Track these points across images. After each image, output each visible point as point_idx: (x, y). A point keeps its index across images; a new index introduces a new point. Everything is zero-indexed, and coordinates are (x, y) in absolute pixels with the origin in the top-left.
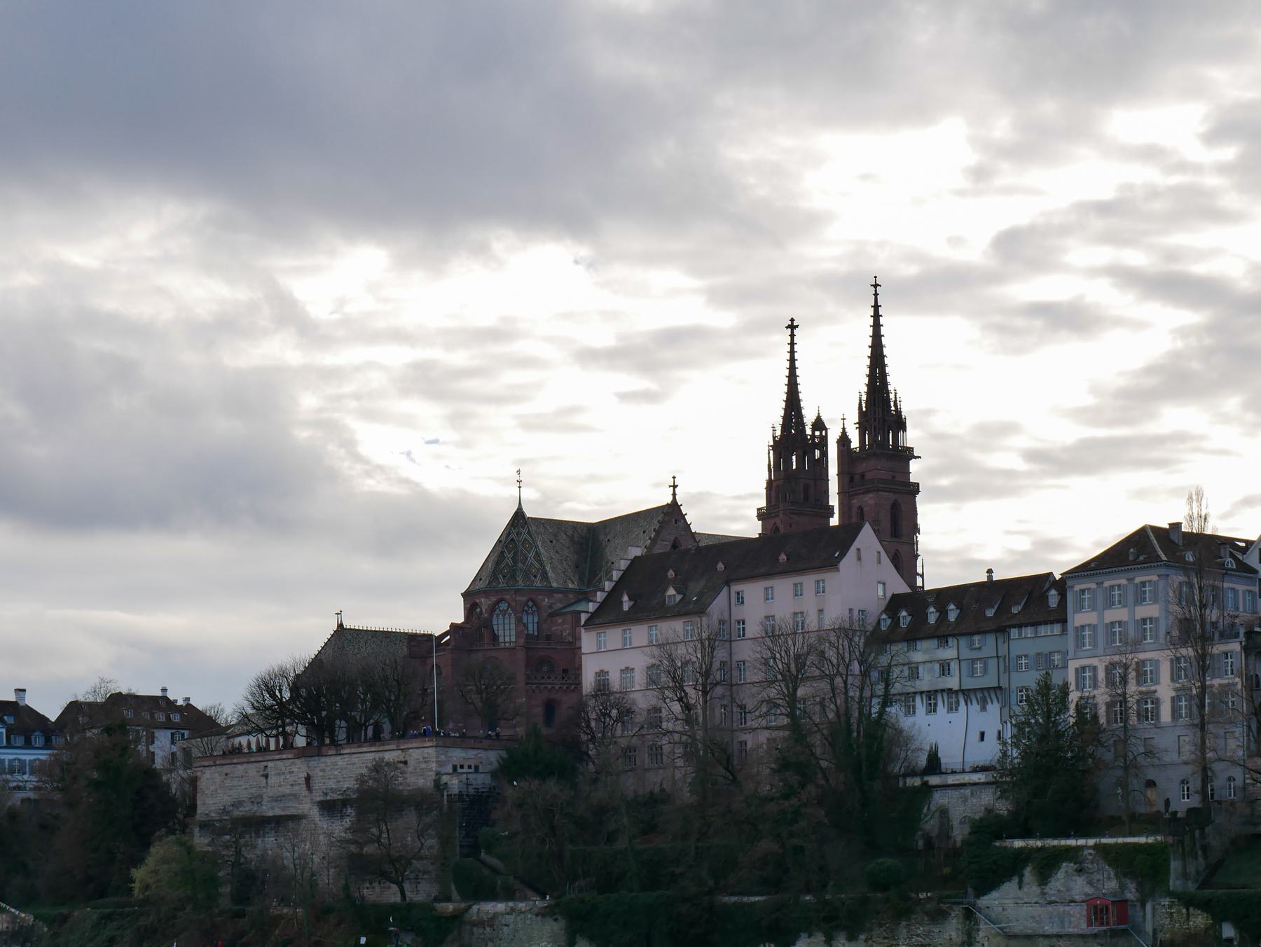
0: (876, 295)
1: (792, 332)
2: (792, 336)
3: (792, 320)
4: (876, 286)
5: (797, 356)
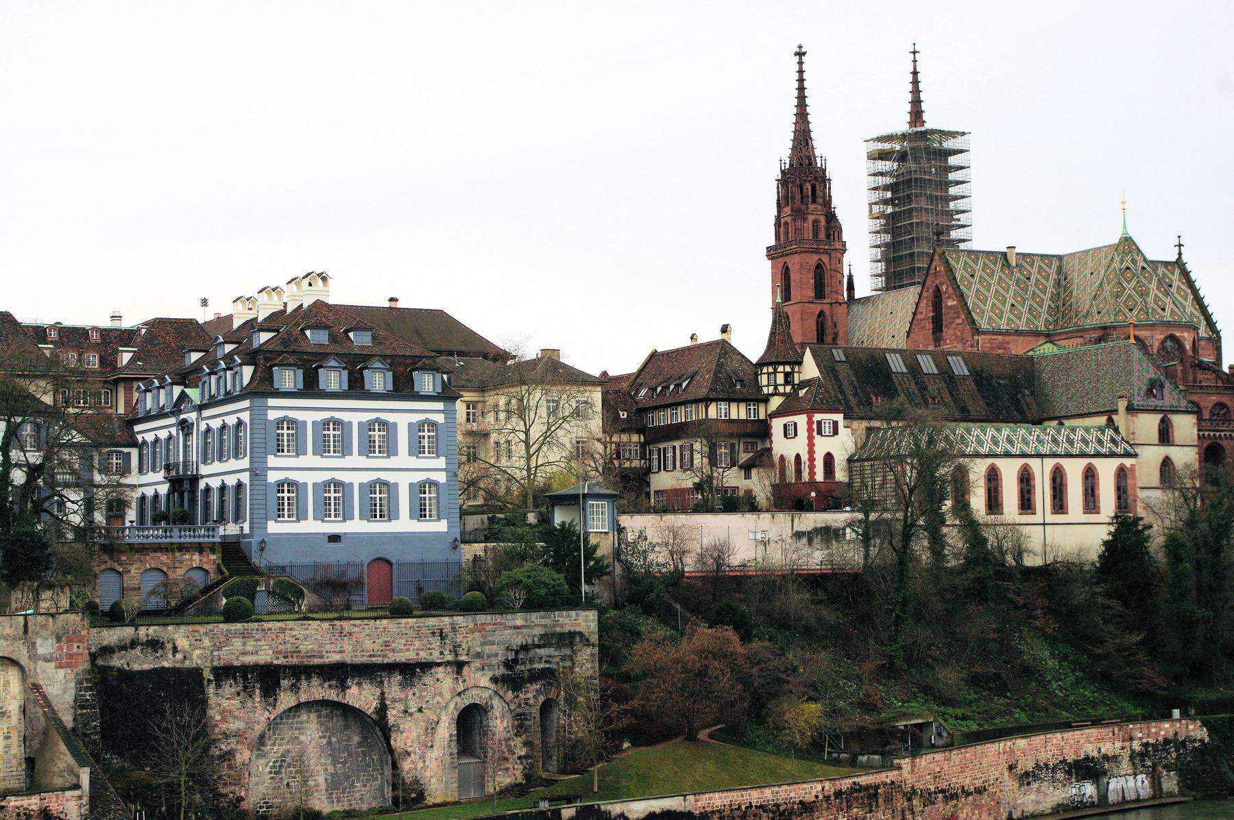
0: (915, 61)
1: (800, 59)
2: (801, 63)
3: (800, 47)
4: (914, 53)
5: (806, 84)
